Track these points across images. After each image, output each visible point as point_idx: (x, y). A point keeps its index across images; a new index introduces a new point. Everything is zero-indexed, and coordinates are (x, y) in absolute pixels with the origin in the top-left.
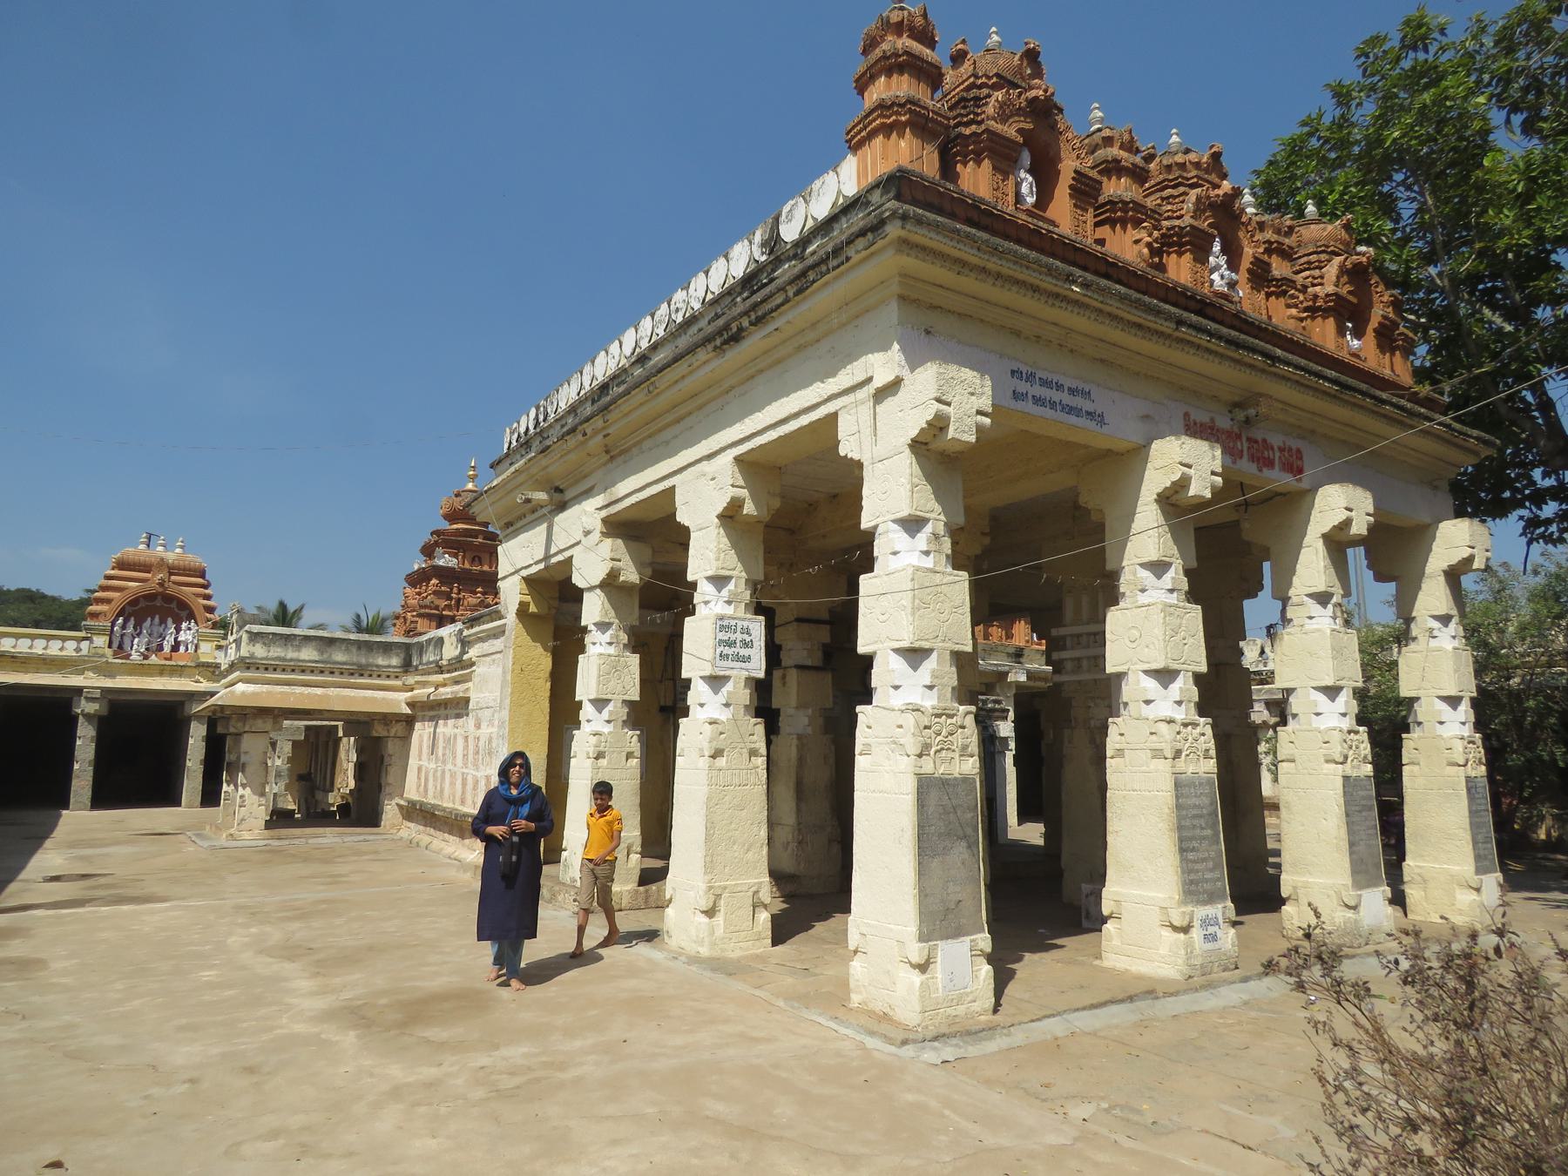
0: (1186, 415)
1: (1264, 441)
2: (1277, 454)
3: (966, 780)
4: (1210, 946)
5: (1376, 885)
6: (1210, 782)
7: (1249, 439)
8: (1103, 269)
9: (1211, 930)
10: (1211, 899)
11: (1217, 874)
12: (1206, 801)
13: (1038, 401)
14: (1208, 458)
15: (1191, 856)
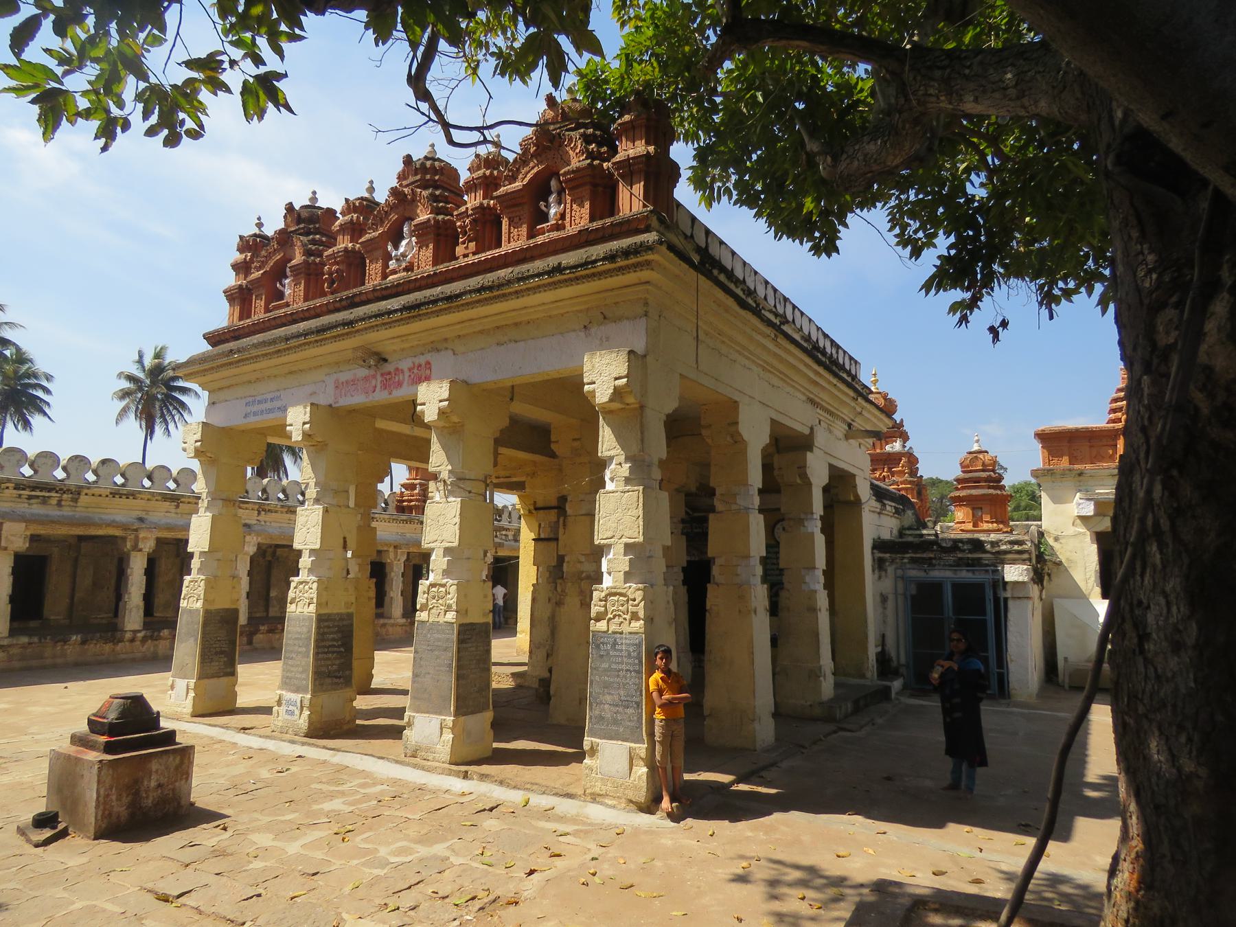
0: (337, 381)
1: (397, 369)
2: (407, 374)
3: (197, 610)
4: (287, 717)
5: (440, 714)
6: (310, 618)
7: (382, 375)
8: (289, 318)
9: (291, 708)
10: (297, 691)
11: (304, 676)
12: (305, 630)
13: (255, 414)
14: (302, 415)
15: (290, 662)
